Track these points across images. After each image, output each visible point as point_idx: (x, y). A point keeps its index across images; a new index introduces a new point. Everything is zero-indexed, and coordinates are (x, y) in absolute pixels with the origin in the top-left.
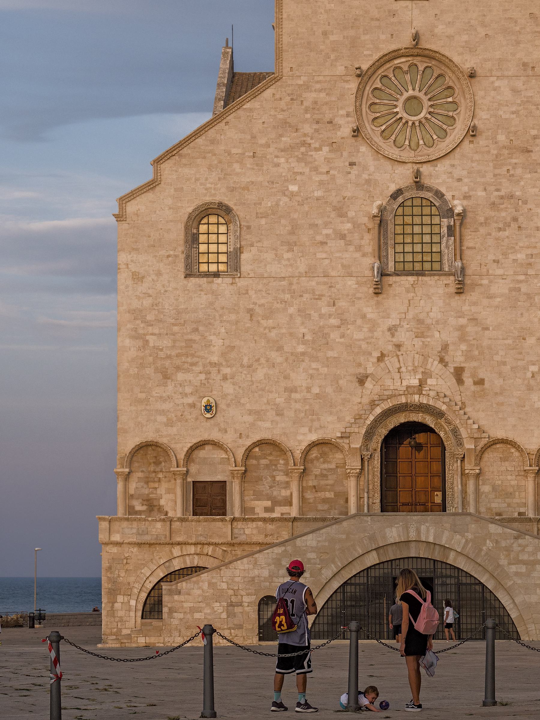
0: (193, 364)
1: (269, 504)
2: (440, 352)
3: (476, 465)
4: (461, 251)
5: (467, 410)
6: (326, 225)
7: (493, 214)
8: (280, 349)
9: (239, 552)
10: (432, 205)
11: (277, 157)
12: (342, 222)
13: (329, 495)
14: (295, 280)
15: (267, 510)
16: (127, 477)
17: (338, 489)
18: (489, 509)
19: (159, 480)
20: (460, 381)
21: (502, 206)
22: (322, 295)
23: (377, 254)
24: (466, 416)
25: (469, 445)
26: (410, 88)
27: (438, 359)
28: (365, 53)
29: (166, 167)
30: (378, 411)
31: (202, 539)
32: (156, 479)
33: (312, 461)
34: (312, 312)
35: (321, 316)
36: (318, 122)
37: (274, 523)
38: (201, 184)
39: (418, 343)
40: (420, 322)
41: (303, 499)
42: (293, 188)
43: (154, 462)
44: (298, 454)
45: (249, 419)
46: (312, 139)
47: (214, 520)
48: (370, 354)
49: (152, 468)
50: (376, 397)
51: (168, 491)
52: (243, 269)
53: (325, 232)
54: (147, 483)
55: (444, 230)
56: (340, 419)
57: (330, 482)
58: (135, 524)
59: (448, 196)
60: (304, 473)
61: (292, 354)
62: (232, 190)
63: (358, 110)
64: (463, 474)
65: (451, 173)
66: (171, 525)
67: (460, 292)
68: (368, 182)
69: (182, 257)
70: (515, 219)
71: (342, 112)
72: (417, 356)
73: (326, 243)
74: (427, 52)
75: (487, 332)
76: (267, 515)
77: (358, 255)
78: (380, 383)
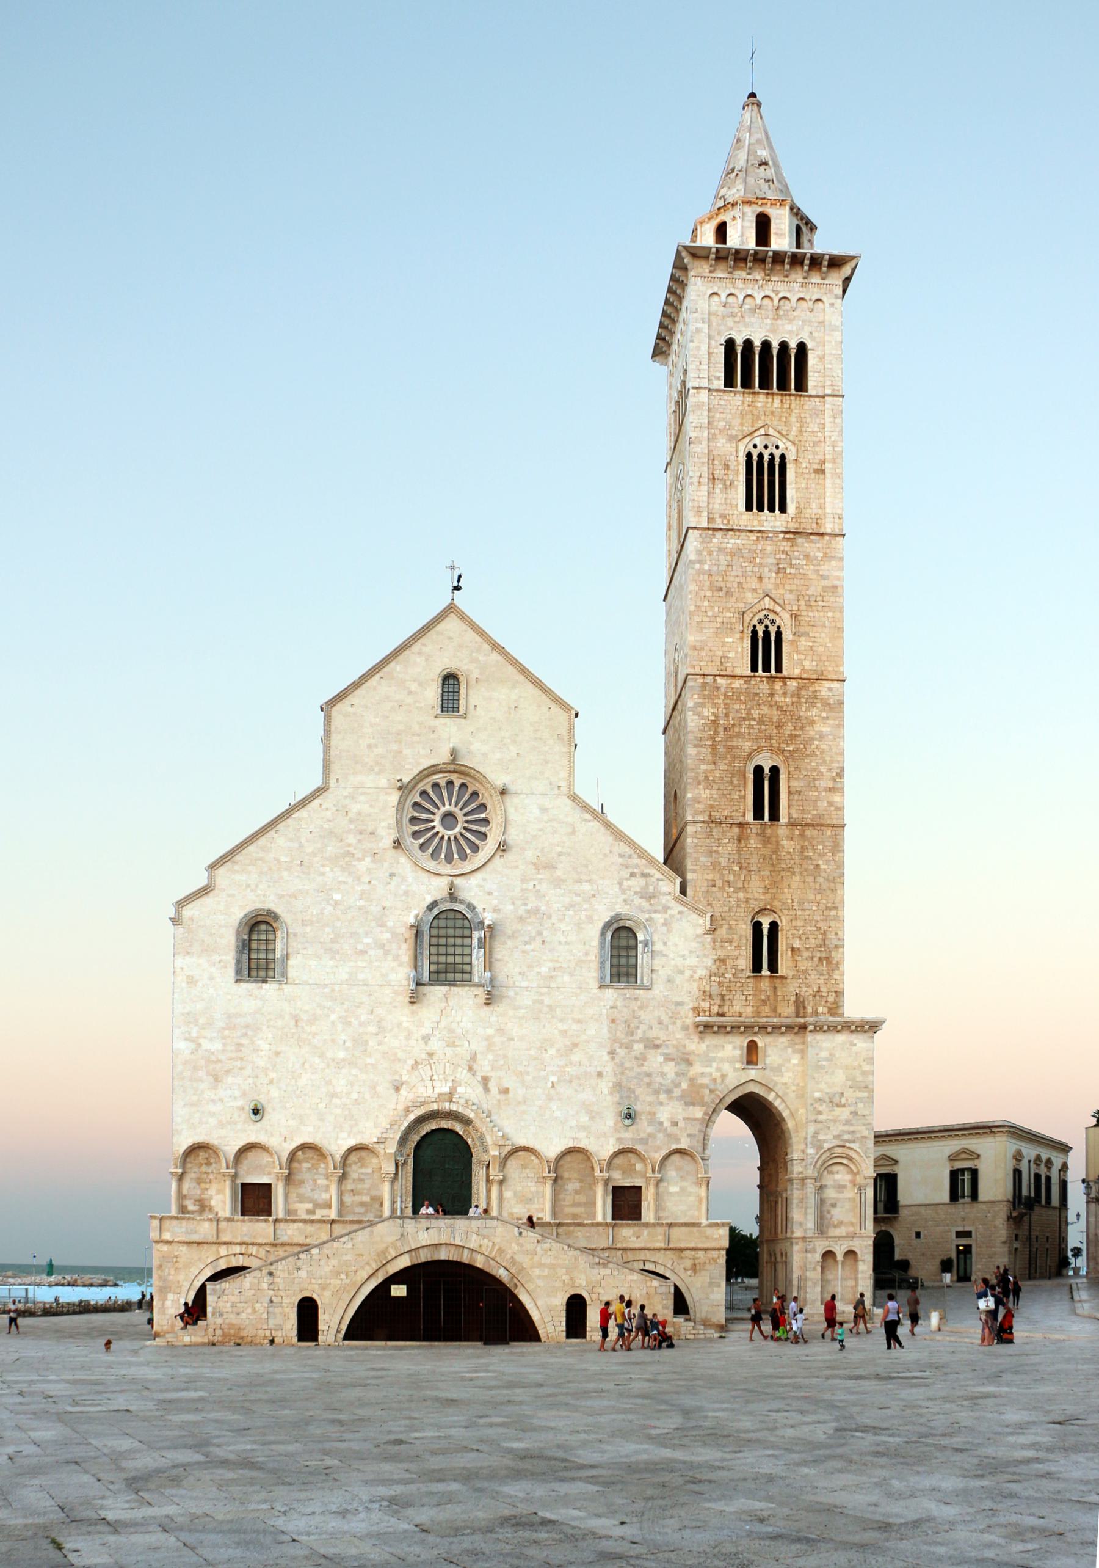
0: (241, 1069)
1: (310, 1206)
2: (468, 1061)
3: (501, 1171)
4: (490, 962)
5: (494, 1117)
6: (367, 934)
7: (519, 927)
8: (322, 1056)
9: (281, 1252)
10: (465, 917)
11: (323, 866)
12: (382, 932)
13: (366, 1199)
14: (337, 988)
15: (309, 1212)
16: (181, 1178)
17: (374, 1193)
18: (512, 1214)
19: (210, 1182)
20: (486, 1089)
22: (361, 1003)
23: (412, 962)
24: (492, 1124)
25: (494, 1152)
26: (447, 803)
28: (407, 767)
29: (221, 871)
30: (412, 1117)
31: (246, 1239)
32: (208, 1180)
33: (350, 1165)
34: (353, 1020)
35: (361, 1024)
36: (361, 833)
37: (314, 1225)
38: (252, 891)
39: (449, 1051)
40: (451, 1031)
41: (341, 1203)
42: (337, 897)
44: (338, 1158)
45: (292, 1123)
46: (355, 849)
47: (258, 1221)
48: (405, 1062)
50: (410, 1104)
51: (219, 1192)
52: (290, 975)
53: (366, 940)
54: (199, 1184)
55: (475, 942)
56: (376, 1126)
57: (366, 1186)
58: (184, 1223)
59: (479, 909)
60: (343, 1177)
61: (333, 1060)
62: (281, 897)
63: (399, 822)
64: (488, 1180)
65: (481, 886)
66: (218, 1225)
68: (406, 893)
69: (233, 962)
70: (540, 933)
71: (384, 824)
72: (447, 1065)
73: (366, 952)
74: (463, 768)
75: (512, 1042)
76: (307, 1217)
77: (395, 964)
78: (414, 1090)
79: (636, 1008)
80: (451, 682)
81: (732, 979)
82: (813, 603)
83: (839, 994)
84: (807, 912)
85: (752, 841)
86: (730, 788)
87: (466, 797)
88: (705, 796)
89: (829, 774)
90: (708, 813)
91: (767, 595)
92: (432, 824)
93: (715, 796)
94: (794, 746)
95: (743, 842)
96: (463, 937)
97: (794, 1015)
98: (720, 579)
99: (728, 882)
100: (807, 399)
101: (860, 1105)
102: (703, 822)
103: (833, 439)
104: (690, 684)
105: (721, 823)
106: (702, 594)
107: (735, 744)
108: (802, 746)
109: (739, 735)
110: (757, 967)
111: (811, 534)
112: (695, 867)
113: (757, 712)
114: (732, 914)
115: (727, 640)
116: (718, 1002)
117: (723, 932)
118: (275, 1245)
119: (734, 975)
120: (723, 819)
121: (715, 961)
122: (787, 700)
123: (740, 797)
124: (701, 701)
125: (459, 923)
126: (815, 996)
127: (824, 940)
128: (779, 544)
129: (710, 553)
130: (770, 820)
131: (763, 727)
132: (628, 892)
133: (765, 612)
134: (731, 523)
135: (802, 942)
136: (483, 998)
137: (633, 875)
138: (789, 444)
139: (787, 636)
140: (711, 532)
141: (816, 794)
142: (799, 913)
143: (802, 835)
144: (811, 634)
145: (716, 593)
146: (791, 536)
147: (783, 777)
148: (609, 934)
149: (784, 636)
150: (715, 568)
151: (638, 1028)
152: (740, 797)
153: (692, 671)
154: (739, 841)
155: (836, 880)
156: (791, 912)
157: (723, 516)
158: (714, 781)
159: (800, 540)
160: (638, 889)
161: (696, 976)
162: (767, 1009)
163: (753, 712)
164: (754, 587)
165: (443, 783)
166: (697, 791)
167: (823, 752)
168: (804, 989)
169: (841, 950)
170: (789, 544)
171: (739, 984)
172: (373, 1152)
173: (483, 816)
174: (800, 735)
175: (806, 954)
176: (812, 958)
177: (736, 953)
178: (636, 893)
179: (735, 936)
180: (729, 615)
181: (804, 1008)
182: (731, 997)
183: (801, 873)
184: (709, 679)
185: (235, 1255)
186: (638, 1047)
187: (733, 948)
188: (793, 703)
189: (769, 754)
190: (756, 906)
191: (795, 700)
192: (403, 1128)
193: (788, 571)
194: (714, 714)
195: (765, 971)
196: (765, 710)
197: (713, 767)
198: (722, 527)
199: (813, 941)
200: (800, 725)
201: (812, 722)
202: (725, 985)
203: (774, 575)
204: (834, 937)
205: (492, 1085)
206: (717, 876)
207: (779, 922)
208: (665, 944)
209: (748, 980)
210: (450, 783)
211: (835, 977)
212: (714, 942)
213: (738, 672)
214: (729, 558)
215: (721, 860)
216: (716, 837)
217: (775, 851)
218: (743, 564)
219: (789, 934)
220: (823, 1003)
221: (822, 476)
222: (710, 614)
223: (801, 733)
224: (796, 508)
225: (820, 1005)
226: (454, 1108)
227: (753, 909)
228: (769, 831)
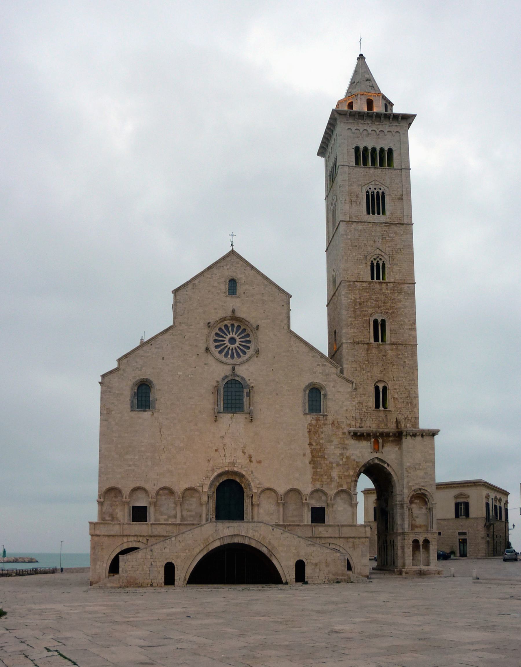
10: (240, 383)
36: (191, 346)
59: (247, 379)
80: (233, 282)
81: (366, 411)
82: (399, 252)
83: (417, 418)
84: (401, 382)
85: (374, 351)
86: (363, 328)
87: (240, 331)
89: (409, 323)
91: (378, 248)
92: (224, 342)
93: (356, 332)
95: (369, 351)
96: (239, 392)
97: (395, 428)
98: (356, 242)
99: (363, 368)
102: (351, 343)
104: (343, 284)
105: (359, 343)
106: (347, 248)
107: (364, 310)
108: (396, 311)
110: (377, 406)
111: (397, 224)
113: (374, 296)
115: (360, 267)
116: (359, 421)
117: (361, 390)
118: (151, 536)
119: (366, 409)
120: (360, 341)
121: (358, 403)
122: (388, 292)
124: (348, 292)
125: (237, 386)
126: (405, 419)
127: (409, 394)
128: (383, 227)
129: (351, 231)
130: (381, 342)
131: (377, 303)
134: (360, 219)
135: (398, 395)
137: (318, 365)
138: (386, 188)
139: (387, 265)
140: (351, 223)
142: (397, 382)
144: (399, 264)
146: (388, 225)
149: (386, 266)
150: (353, 237)
153: (344, 279)
155: (414, 368)
156: (393, 382)
158: (354, 325)
159: (393, 226)
160: (321, 371)
163: (372, 296)
165: (229, 325)
166: (347, 330)
167: (405, 313)
169: (417, 399)
171: (369, 414)
172: (198, 491)
173: (248, 339)
174: (395, 307)
175: (401, 401)
177: (368, 399)
178: (320, 373)
180: (360, 256)
181: (401, 425)
182: (365, 419)
184: (352, 283)
185: (131, 542)
187: (366, 397)
188: (391, 293)
189: (381, 314)
192: (211, 479)
195: (381, 408)
196: (378, 296)
197: (354, 319)
199: (404, 395)
200: (395, 302)
201: (400, 301)
203: (381, 240)
204: (414, 393)
210: (233, 325)
211: (415, 411)
213: (365, 280)
214: (359, 233)
216: (357, 349)
218: (366, 236)
219: (392, 392)
220: (409, 422)
221: (401, 201)
222: (351, 256)
223: (395, 305)
224: (390, 213)
225: (408, 423)
226: (236, 469)
228: (381, 347)
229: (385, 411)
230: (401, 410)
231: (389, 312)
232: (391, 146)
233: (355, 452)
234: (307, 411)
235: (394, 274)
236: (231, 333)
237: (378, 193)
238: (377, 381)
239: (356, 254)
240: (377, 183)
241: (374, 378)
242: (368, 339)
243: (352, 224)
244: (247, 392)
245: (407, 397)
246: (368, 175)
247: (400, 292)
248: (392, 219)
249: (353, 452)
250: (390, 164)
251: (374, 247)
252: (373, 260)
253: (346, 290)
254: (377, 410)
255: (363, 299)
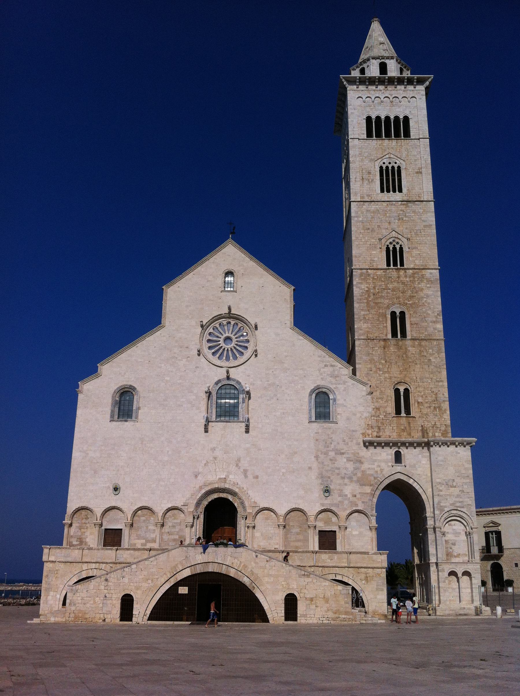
20: (246, 476)
21: (269, 389)
27: (236, 465)
43: (85, 518)
49: (84, 521)
59: (243, 384)
67: (247, 431)
70: (276, 395)
72: (225, 463)
79: (330, 433)
81: (384, 418)
85: (392, 348)
87: (231, 328)
88: (364, 327)
90: (366, 335)
91: (394, 230)
93: (370, 327)
94: (412, 301)
99: (379, 368)
100: (410, 140)
101: (465, 487)
102: (364, 339)
103: (425, 157)
105: (373, 339)
106: (359, 231)
107: (379, 301)
108: (417, 301)
109: (382, 297)
110: (398, 411)
111: (416, 201)
112: (360, 362)
113: (391, 286)
114: (382, 385)
115: (373, 252)
116: (377, 430)
117: (377, 394)
119: (385, 416)
120: (375, 338)
121: (374, 409)
122: (407, 279)
123: (384, 327)
127: (436, 398)
131: (395, 293)
132: (324, 374)
133: (393, 239)
135: (424, 399)
136: (243, 429)
137: (326, 366)
138: (402, 161)
139: (405, 249)
141: (426, 324)
142: (421, 384)
143: (420, 345)
145: (366, 231)
147: (407, 316)
148: (314, 395)
151: (331, 443)
152: (384, 327)
154: (384, 348)
156: (416, 384)
157: (368, 196)
158: (368, 320)
159: (410, 204)
161: (363, 417)
162: (405, 434)
163: (388, 285)
164: (386, 227)
166: (360, 324)
168: (426, 423)
170: (405, 206)
171: (388, 421)
175: (426, 405)
176: (430, 407)
177: (386, 404)
178: (328, 375)
179: (384, 396)
180: (373, 240)
181: (427, 433)
183: (420, 364)
186: (332, 454)
190: (396, 380)
191: (412, 279)
193: (404, 219)
194: (367, 287)
195: (403, 414)
196: (395, 284)
198: (368, 200)
199: (430, 398)
201: (422, 290)
202: (380, 421)
203: (397, 221)
205: (249, 473)
206: (373, 366)
207: (409, 389)
208: (345, 400)
209: (394, 419)
212: (373, 399)
213: (379, 267)
214: (372, 215)
215: (375, 358)
216: (371, 346)
217: (405, 353)
218: (380, 217)
219: (416, 395)
221: (420, 175)
223: (416, 295)
224: (407, 190)
227: (394, 382)
228: (400, 343)
229: (408, 417)
230: (428, 417)
231: (409, 303)
232: (407, 113)
233: (373, 466)
234: (313, 419)
235: (413, 259)
236: (227, 332)
237: (393, 167)
238: (396, 383)
239: (369, 238)
240: (392, 156)
241: (394, 380)
242: (384, 335)
243: (364, 205)
244: (242, 398)
245: (434, 401)
246: (381, 148)
247: (421, 279)
248: (409, 197)
249: (370, 466)
250: (407, 134)
251: (389, 229)
252: (389, 244)
253: (357, 279)
254: (398, 417)
255: (378, 290)
